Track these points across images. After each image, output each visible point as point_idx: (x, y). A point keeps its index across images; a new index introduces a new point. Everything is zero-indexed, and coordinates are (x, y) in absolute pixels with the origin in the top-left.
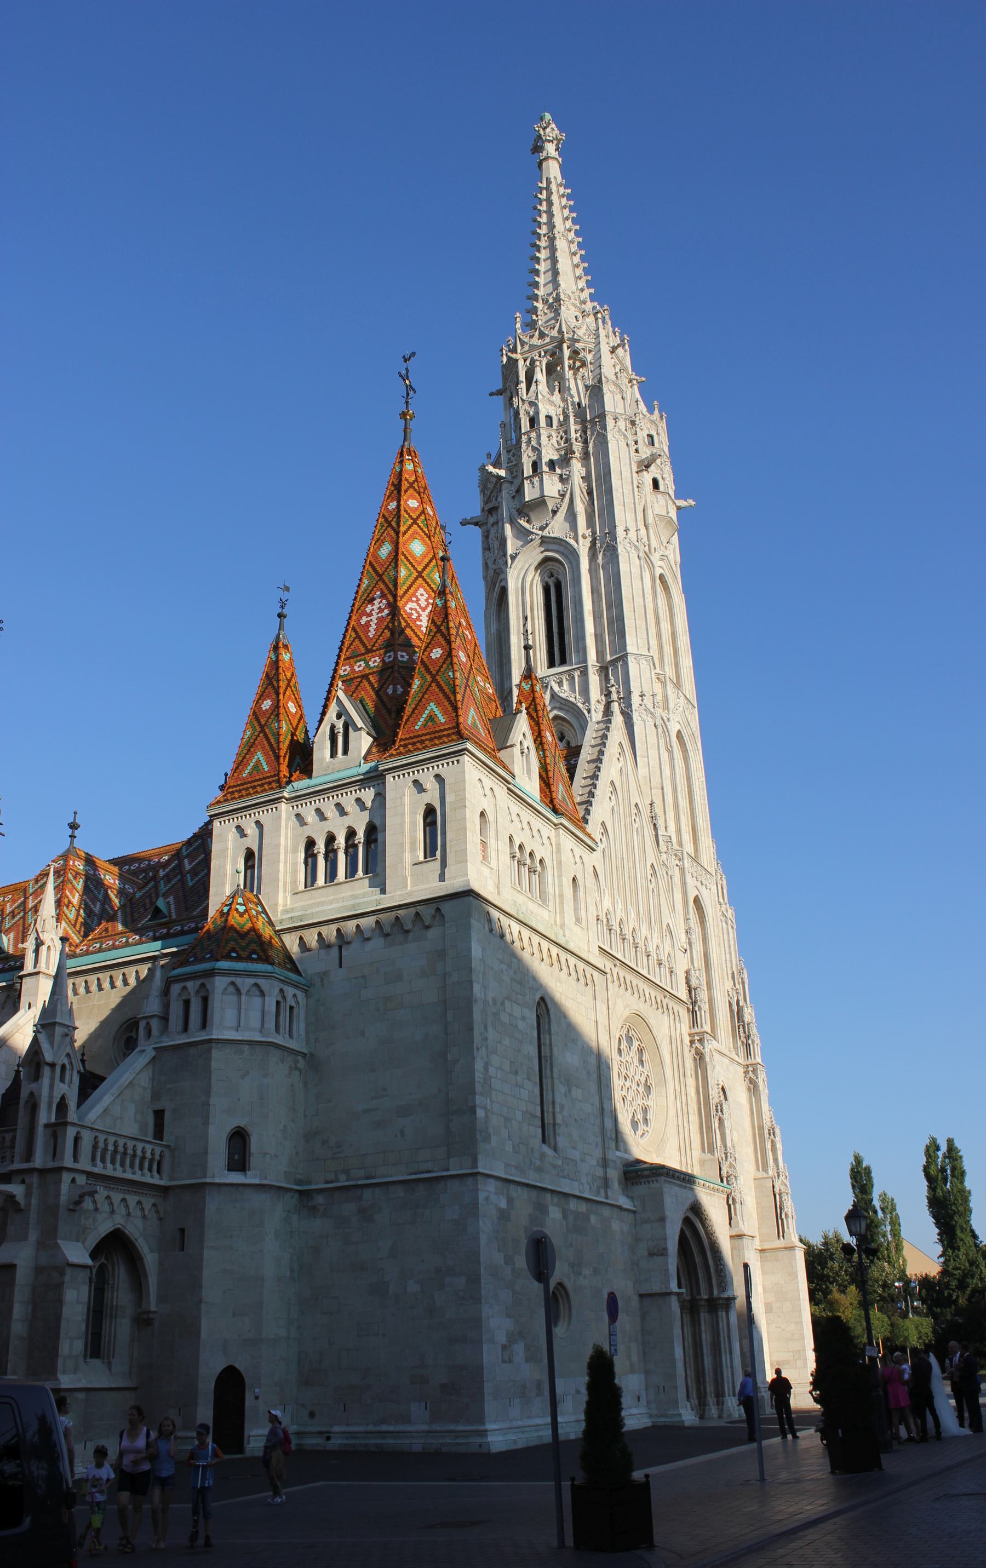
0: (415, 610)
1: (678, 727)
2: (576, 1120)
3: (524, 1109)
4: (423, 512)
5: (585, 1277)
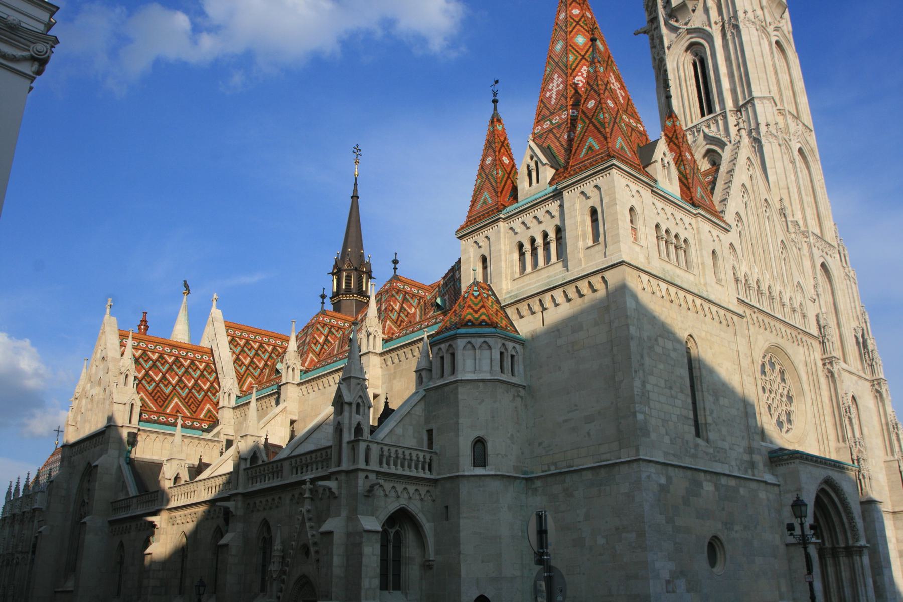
0: (581, 81)
1: (799, 146)
2: (724, 421)
3: (678, 413)
4: (583, 16)
5: (737, 532)
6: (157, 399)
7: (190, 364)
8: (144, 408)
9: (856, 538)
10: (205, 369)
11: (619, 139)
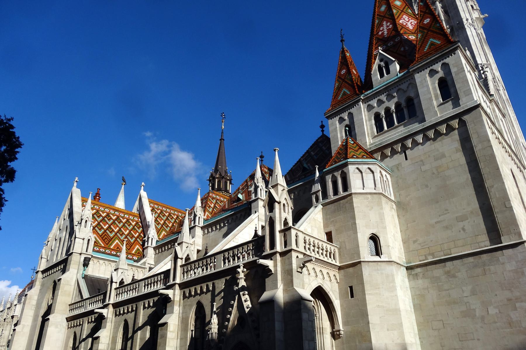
6: (105, 239)
7: (126, 222)
8: (96, 244)
10: (135, 225)
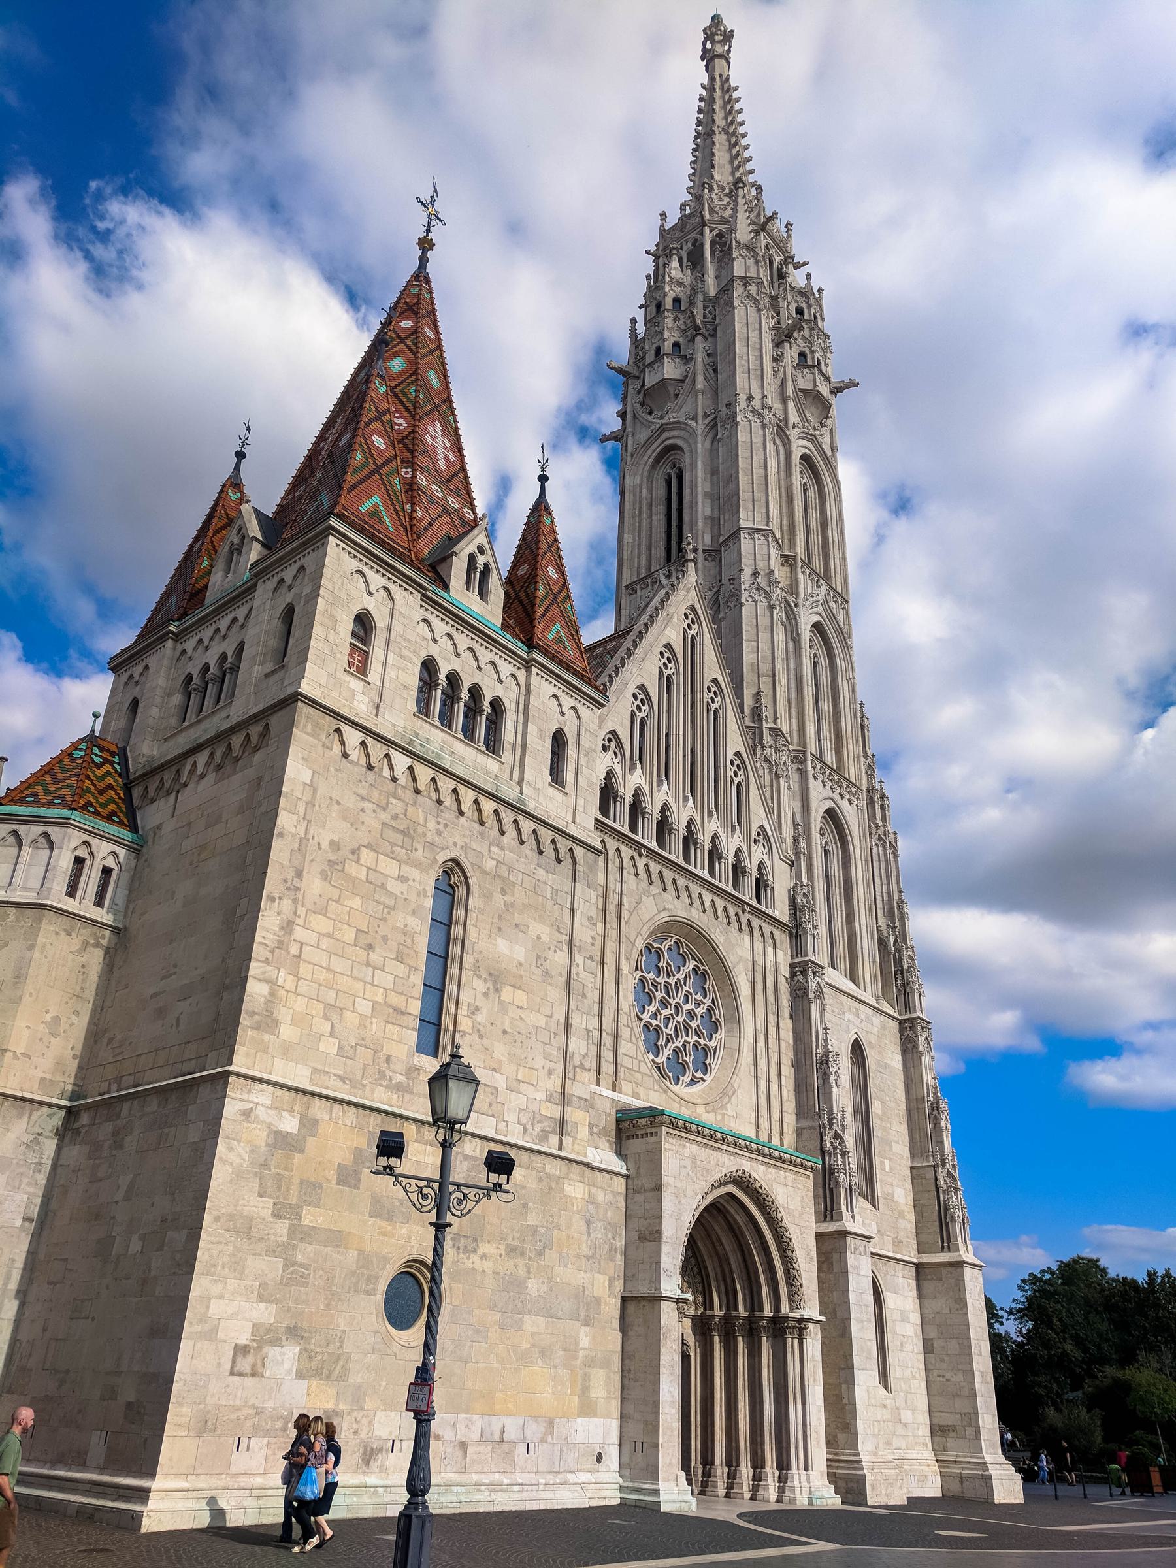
2: (505, 1032)
3: (379, 998)
5: (484, 1257)
9: (795, 1301)
11: (376, 499)
